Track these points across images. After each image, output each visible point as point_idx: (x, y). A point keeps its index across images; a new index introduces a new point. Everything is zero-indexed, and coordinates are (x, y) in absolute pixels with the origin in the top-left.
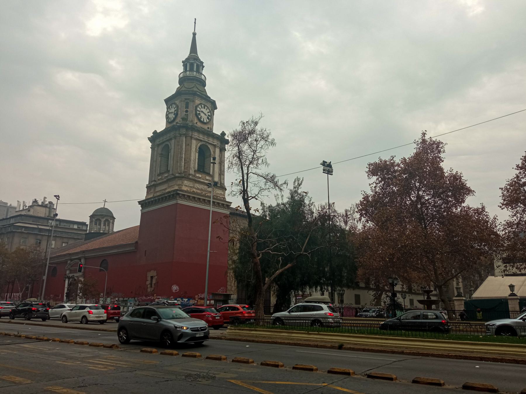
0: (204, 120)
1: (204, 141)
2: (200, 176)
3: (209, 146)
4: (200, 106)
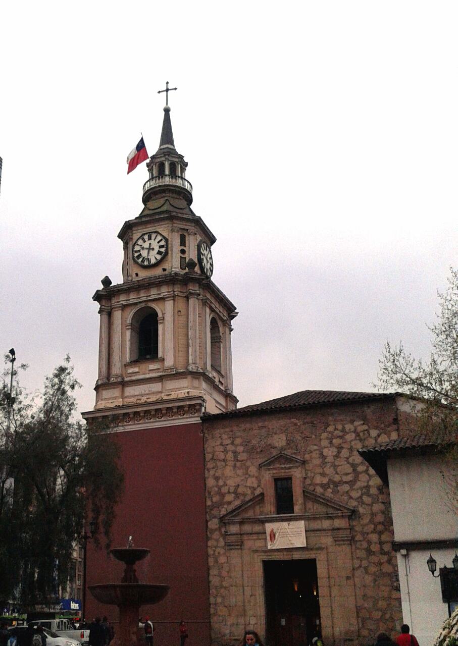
1: (140, 302)
2: (136, 370)
4: (140, 242)
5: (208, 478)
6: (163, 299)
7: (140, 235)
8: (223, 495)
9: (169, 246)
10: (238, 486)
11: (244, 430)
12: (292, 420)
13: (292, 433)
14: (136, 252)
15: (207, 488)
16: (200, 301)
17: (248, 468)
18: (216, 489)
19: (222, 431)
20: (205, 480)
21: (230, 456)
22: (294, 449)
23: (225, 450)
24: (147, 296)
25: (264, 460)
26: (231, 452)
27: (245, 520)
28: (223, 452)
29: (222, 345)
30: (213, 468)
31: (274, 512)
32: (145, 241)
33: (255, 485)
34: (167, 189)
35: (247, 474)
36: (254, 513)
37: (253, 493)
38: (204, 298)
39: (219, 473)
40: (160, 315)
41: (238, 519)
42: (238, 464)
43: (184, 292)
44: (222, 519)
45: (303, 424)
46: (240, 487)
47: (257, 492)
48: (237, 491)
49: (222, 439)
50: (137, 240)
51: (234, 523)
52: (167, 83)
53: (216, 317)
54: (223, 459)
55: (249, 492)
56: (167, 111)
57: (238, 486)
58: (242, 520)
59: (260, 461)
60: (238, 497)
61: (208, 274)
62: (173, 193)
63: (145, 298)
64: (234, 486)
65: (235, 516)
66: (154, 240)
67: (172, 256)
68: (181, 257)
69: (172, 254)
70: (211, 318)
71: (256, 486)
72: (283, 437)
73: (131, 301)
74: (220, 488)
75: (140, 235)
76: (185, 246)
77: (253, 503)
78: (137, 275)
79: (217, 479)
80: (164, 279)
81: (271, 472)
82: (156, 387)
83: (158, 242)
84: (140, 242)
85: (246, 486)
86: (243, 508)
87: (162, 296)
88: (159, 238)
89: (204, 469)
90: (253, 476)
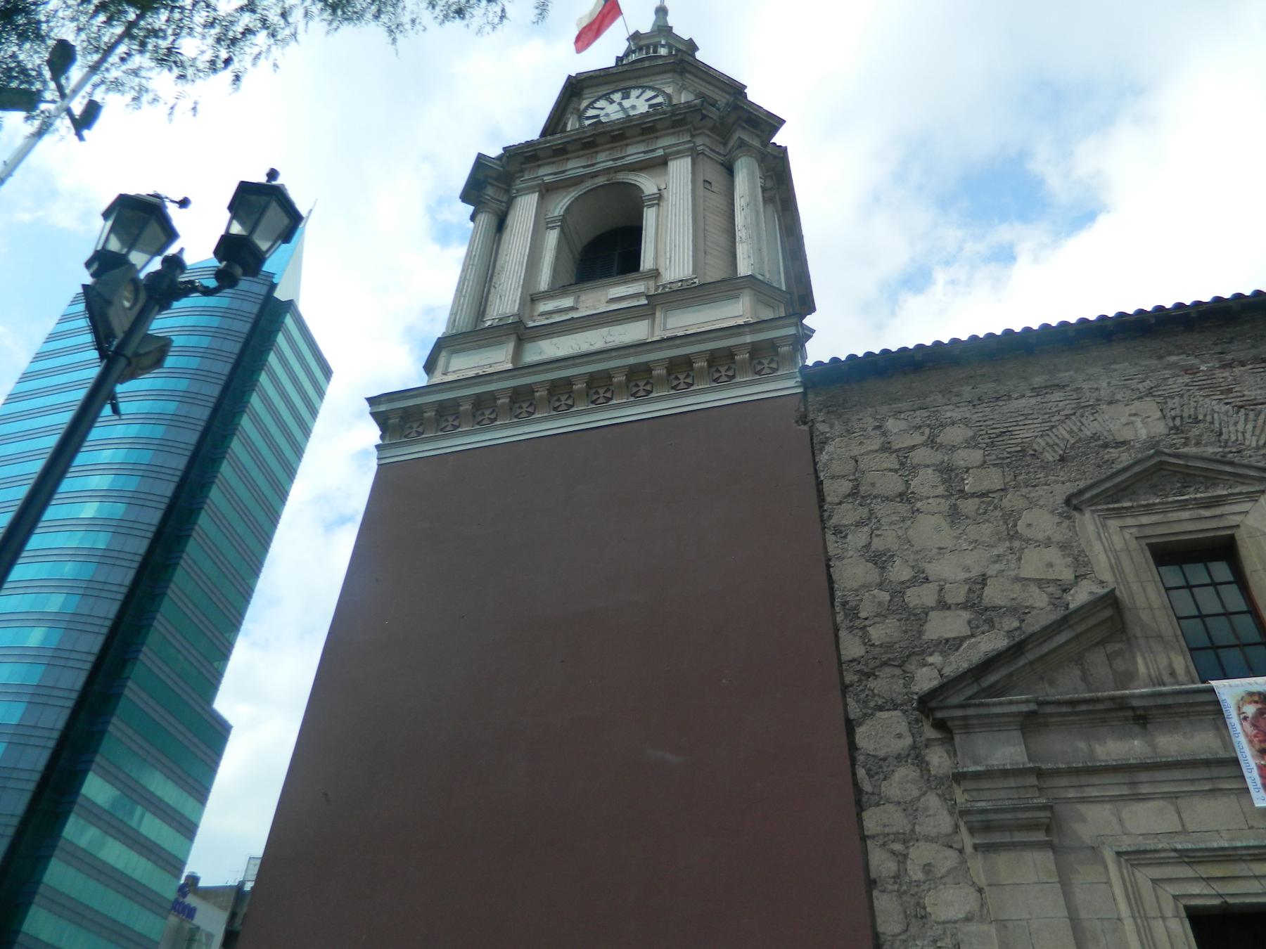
3: (633, 178)
5: (840, 558)
8: (919, 617)
10: (983, 580)
11: (975, 402)
12: (1173, 359)
13: (1182, 396)
15: (838, 594)
17: (1011, 517)
18: (885, 597)
19: (884, 409)
20: (829, 567)
21: (926, 482)
22: (1212, 444)
23: (902, 464)
24: (614, 160)
25: (1082, 484)
26: (930, 471)
27: (1049, 709)
28: (896, 471)
30: (860, 524)
31: (1188, 672)
33: (1067, 575)
35: (1013, 536)
36: (1084, 678)
37: (1054, 602)
39: (887, 540)
41: (1018, 701)
42: (969, 506)
43: (718, 153)
44: (927, 705)
45: (1223, 367)
46: (988, 582)
47: (1081, 596)
48: (980, 596)
49: (884, 434)
50: (594, 102)
51: (992, 724)
54: (901, 495)
55: (1039, 599)
57: (983, 580)
58: (1033, 707)
59: (1070, 488)
60: (991, 623)
63: (611, 163)
64: (966, 581)
65: (994, 691)
71: (1072, 577)
72: (1150, 408)
73: (570, 173)
74: (898, 591)
77: (1077, 637)
79: (880, 560)
81: (1130, 521)
82: (635, 332)
85: (1018, 579)
86: (1030, 656)
89: (824, 528)
90: (1048, 543)
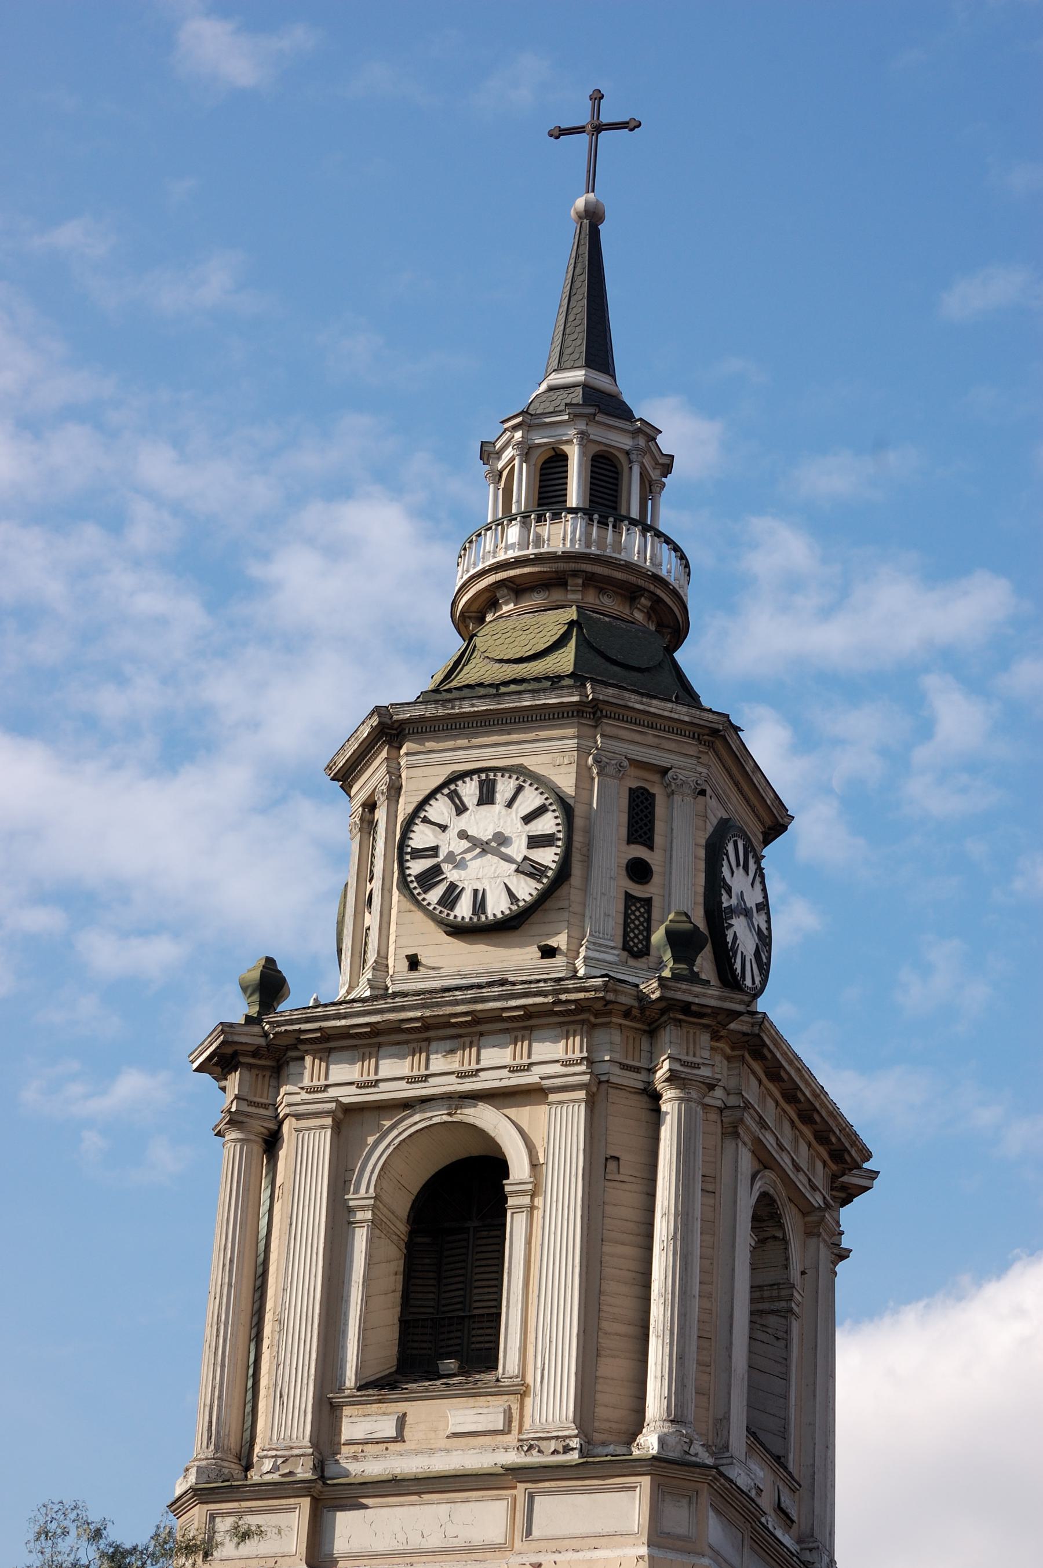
0: (479, 904)
1: (425, 1101)
4: (440, 809)
6: (534, 1094)
7: (440, 780)
9: (578, 838)
14: (417, 854)
16: (713, 1116)
29: (795, 1326)
32: (461, 809)
34: (575, 573)
38: (732, 1101)
40: (519, 1169)
52: (597, 97)
53: (781, 1194)
56: (593, 217)
61: (748, 982)
62: (601, 591)
66: (510, 804)
67: (585, 890)
68: (629, 897)
69: (587, 878)
70: (756, 1195)
75: (440, 775)
76: (651, 848)
78: (414, 963)
80: (550, 999)
83: (528, 819)
84: (440, 809)
87: (530, 1078)
88: (531, 799)
